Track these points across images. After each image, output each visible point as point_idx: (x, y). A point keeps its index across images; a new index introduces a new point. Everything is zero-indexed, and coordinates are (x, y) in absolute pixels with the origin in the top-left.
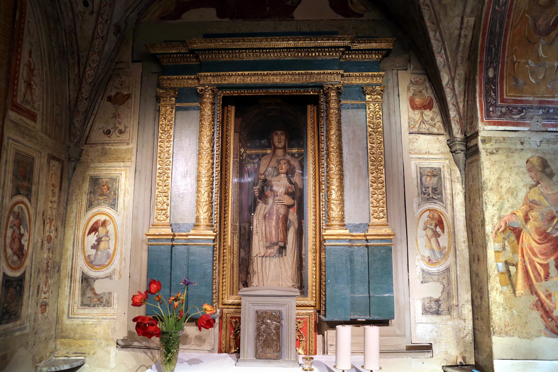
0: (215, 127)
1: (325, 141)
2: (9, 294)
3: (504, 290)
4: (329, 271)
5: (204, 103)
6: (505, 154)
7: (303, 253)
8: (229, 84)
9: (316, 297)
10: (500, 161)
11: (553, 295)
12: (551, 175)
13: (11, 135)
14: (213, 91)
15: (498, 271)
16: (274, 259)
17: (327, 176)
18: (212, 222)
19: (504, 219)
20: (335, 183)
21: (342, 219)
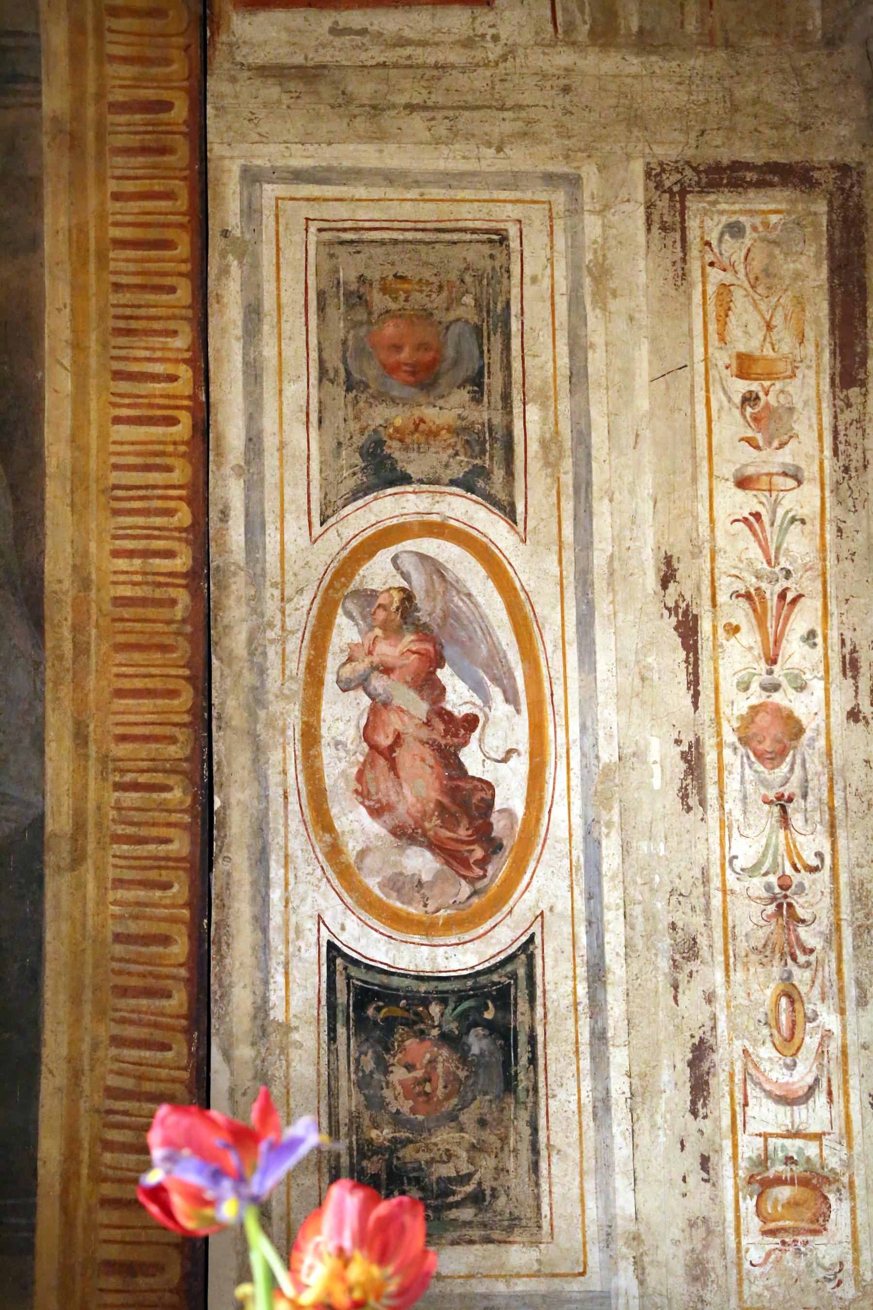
2: (399, 1074)
13: (265, 156)
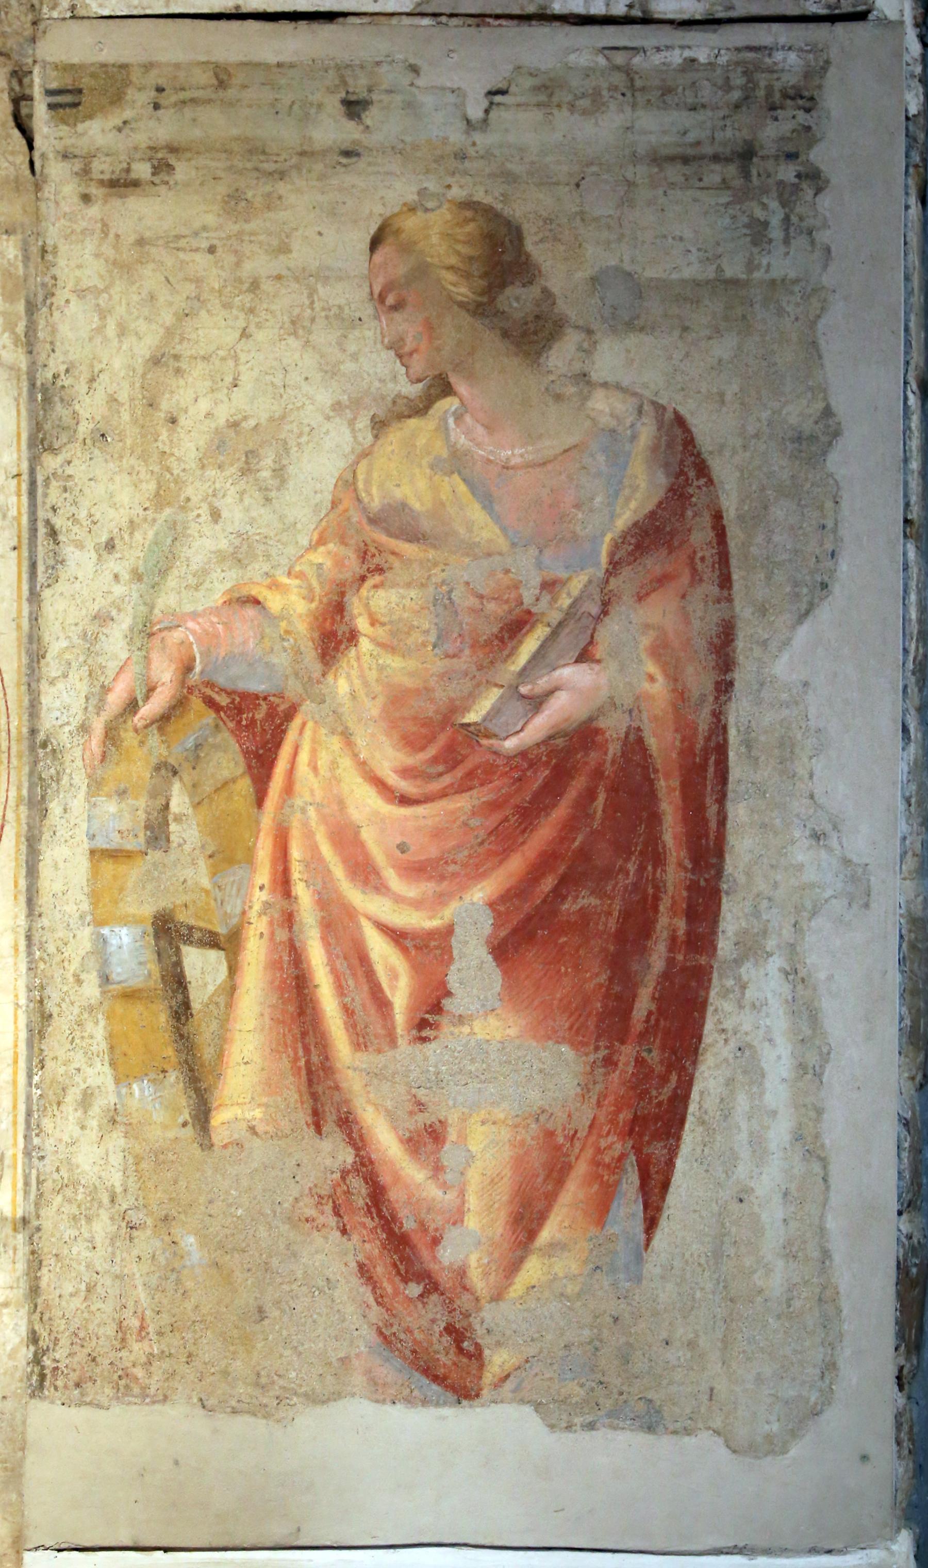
3: (134, 1103)
6: (222, 189)
10: (174, 242)
11: (452, 1135)
12: (532, 336)
15: (105, 979)
19: (177, 635)
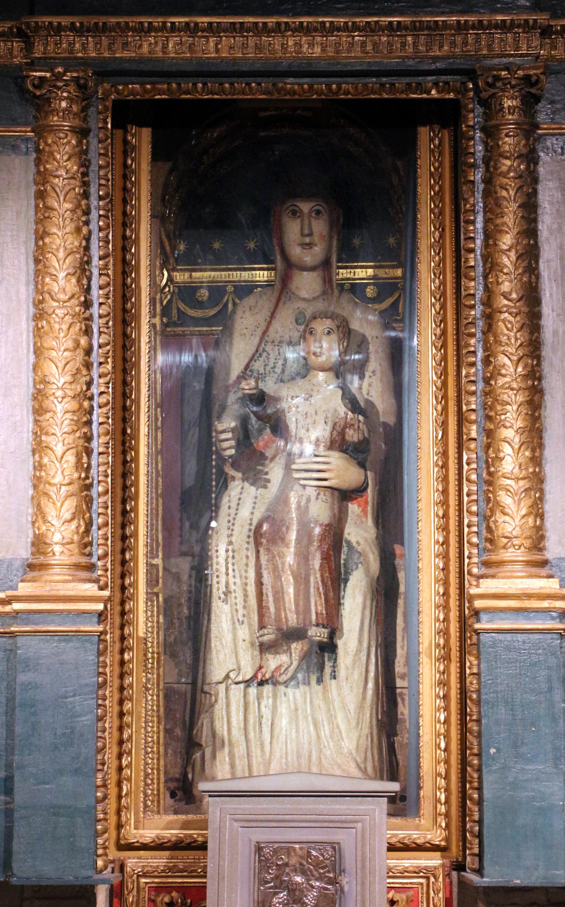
0: (94, 215)
1: (480, 269)
4: (495, 720)
5: (53, 129)
7: (399, 667)
8: (141, 60)
9: (447, 815)
14: (82, 87)
16: (290, 691)
17: (486, 394)
18: (90, 555)
20: (511, 431)
21: (538, 540)
